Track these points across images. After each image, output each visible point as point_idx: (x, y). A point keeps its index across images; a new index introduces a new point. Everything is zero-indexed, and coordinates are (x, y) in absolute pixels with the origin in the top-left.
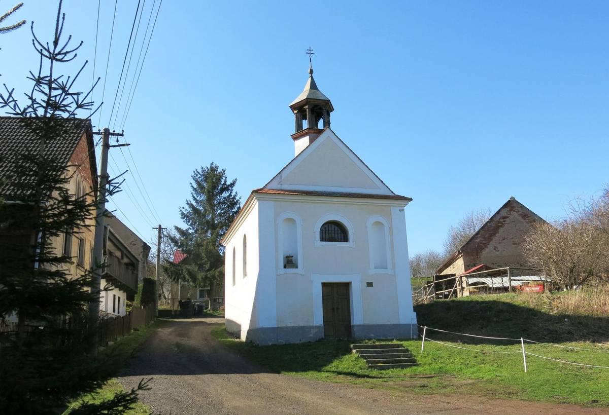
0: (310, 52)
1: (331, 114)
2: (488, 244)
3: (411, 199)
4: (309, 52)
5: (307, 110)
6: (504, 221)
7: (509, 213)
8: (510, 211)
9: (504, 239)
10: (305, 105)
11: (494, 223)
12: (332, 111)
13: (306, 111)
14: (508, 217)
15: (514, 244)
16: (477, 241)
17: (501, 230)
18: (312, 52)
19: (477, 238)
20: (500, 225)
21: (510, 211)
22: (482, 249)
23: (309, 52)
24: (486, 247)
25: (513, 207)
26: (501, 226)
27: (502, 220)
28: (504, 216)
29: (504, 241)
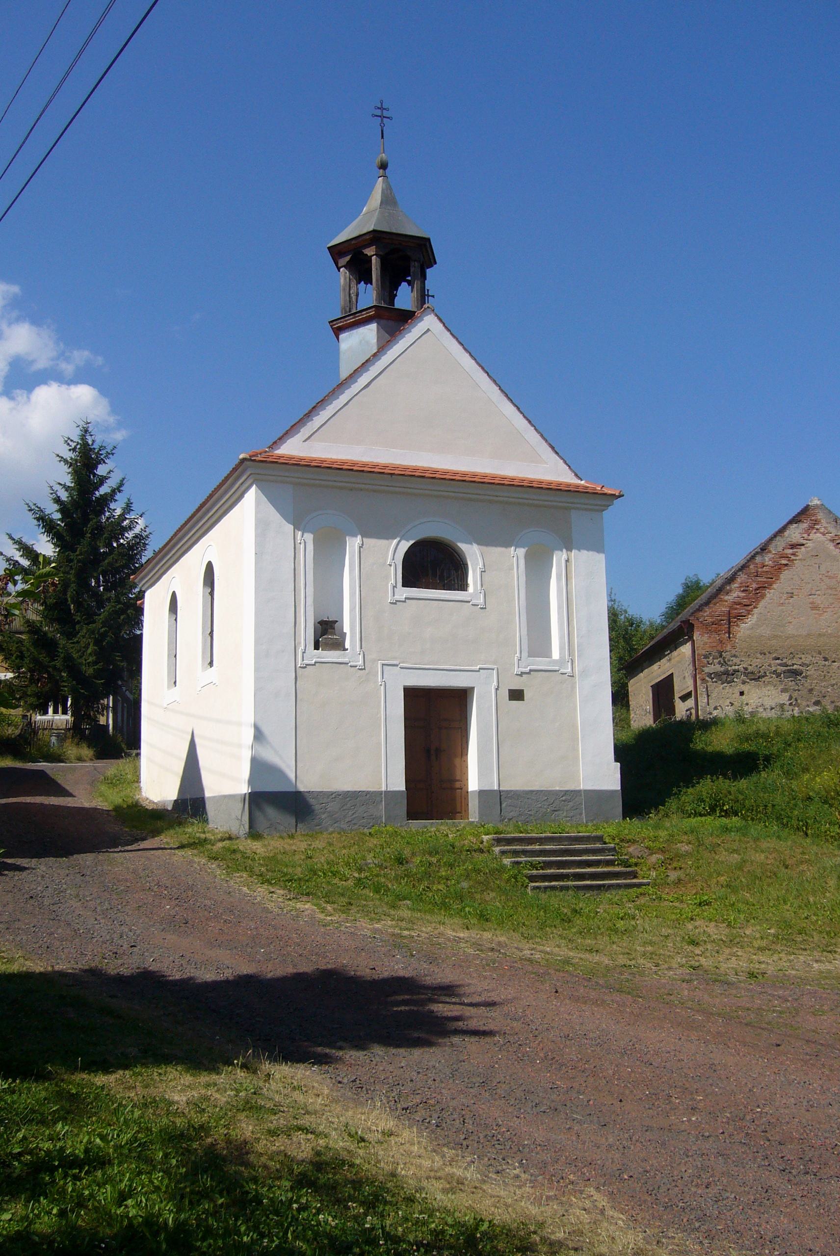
0: (382, 114)
1: (429, 272)
2: (755, 607)
3: (337, 621)
4: (378, 112)
5: (374, 258)
6: (793, 554)
7: (805, 536)
8: (808, 531)
9: (791, 595)
10: (368, 246)
11: (770, 555)
12: (431, 266)
13: (103, 582)
14: (803, 545)
15: (813, 608)
16: (730, 598)
17: (785, 575)
18: (385, 113)
19: (730, 591)
20: (784, 562)
21: (808, 531)
22: (740, 617)
23: (378, 112)
24: (749, 612)
25: (817, 522)
26: (786, 565)
27: (791, 551)
28: (794, 541)
29: (791, 600)
